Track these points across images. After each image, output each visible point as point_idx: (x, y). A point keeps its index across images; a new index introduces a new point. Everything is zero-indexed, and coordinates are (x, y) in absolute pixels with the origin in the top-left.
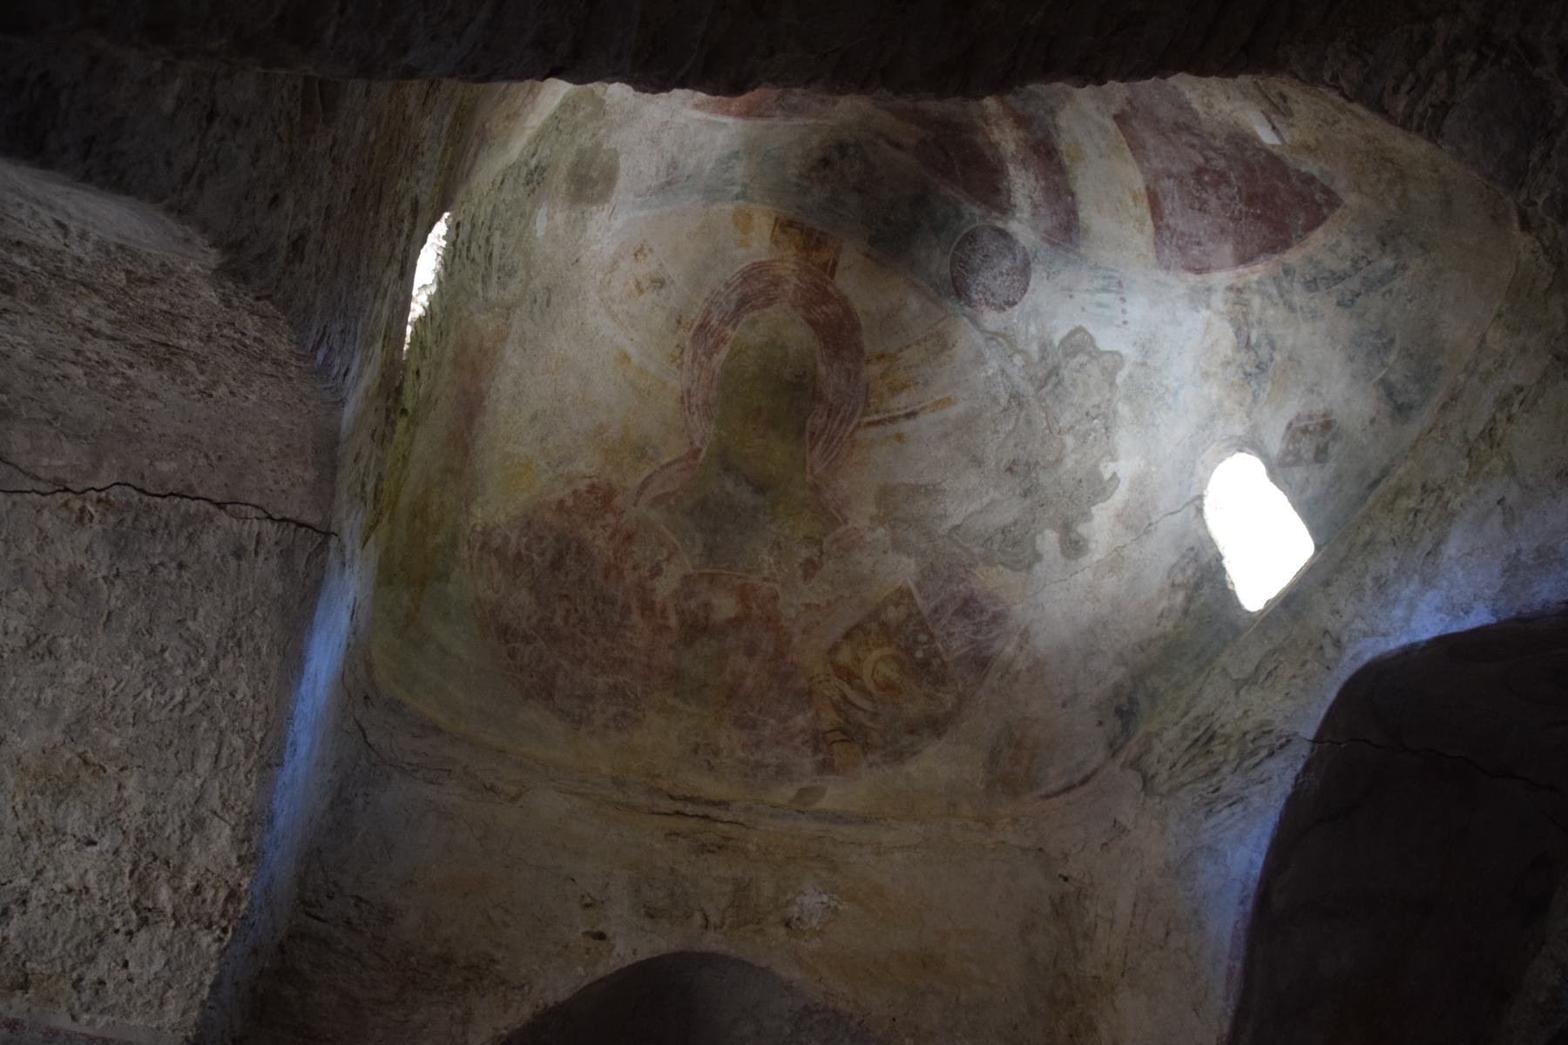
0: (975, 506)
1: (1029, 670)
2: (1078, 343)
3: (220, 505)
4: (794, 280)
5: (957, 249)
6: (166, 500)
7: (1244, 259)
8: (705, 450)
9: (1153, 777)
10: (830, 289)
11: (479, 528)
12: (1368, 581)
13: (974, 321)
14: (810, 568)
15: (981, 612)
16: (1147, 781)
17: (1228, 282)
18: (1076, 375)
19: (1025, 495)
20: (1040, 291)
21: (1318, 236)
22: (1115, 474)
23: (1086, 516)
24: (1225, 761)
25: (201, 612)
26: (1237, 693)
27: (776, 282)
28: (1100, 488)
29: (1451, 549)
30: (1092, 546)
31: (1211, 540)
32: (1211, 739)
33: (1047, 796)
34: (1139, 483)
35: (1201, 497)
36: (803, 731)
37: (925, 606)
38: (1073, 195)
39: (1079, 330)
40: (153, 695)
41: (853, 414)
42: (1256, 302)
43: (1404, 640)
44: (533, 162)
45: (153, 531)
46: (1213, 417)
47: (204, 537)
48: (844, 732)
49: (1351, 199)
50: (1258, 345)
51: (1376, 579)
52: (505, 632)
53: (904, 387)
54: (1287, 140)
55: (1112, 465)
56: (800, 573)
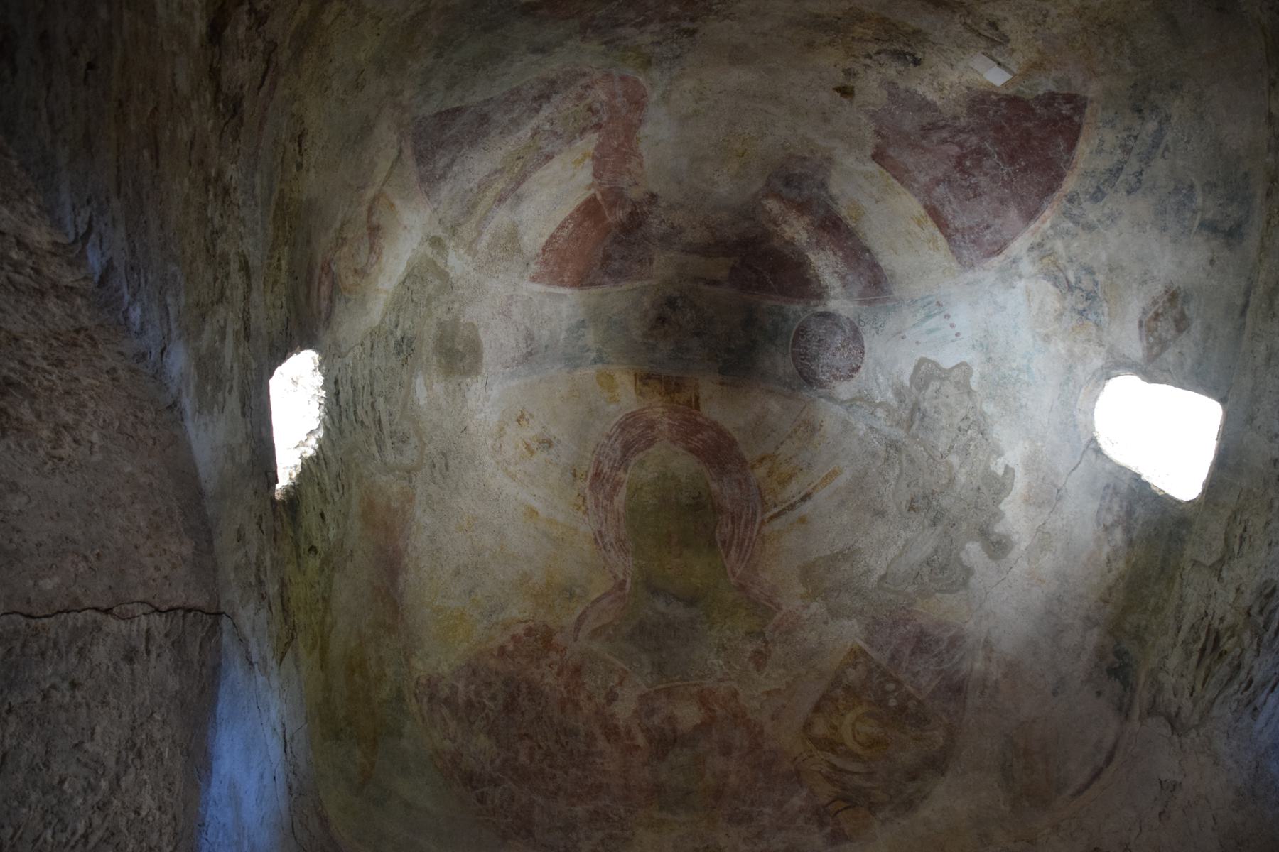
0: (893, 551)
1: (1005, 676)
2: (927, 373)
3: (108, 611)
4: (666, 420)
5: (793, 346)
6: (53, 619)
7: (1031, 215)
8: (629, 580)
9: (1177, 714)
10: (699, 419)
11: (423, 681)
13: (830, 398)
14: (760, 659)
15: (937, 642)
16: (1174, 721)
17: (1028, 245)
18: (935, 402)
19: (934, 523)
20: (876, 346)
21: (1083, 148)
22: (1007, 466)
23: (998, 515)
24: (1243, 650)
25: (98, 730)
26: (1220, 578)
27: (651, 425)
28: (998, 486)
30: (1015, 537)
31: (1122, 467)
32: (1217, 640)
33: (1080, 792)
34: (1032, 463)
35: (1094, 440)
36: (802, 810)
37: (881, 657)
38: (868, 250)
39: (922, 361)
40: (53, 837)
41: (754, 514)
42: (1059, 245)
44: (399, 333)
45: (43, 654)
46: (1070, 368)
47: (95, 648)
48: (845, 800)
49: (1093, 90)
50: (1079, 281)
52: (470, 780)
53: (791, 477)
54: (1015, 71)
55: (1000, 461)
56: (751, 666)
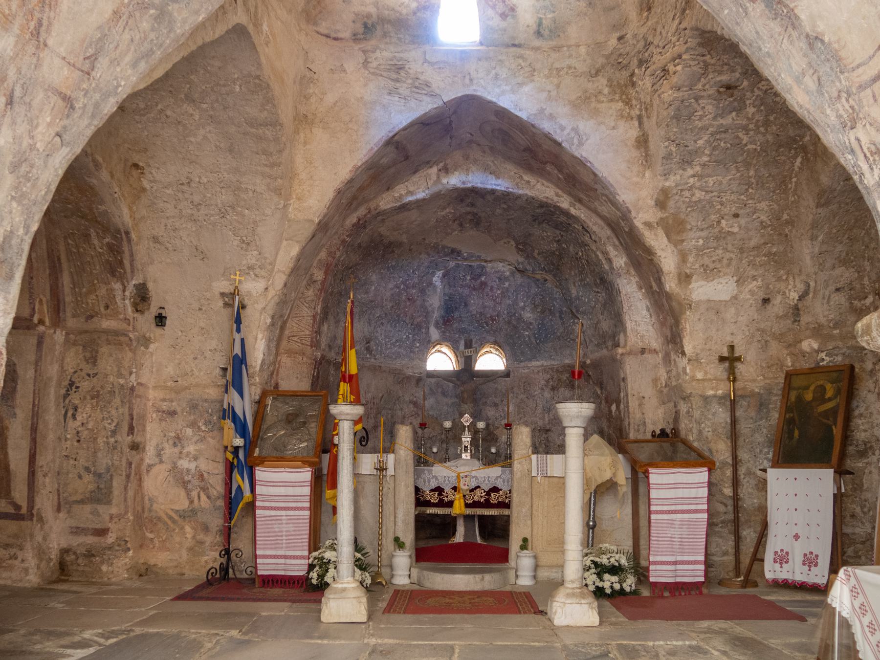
12: (494, 72)
16: (366, 63)
26: (423, 64)
29: (526, 89)
33: (318, 33)
43: (494, 100)
51: (497, 75)
